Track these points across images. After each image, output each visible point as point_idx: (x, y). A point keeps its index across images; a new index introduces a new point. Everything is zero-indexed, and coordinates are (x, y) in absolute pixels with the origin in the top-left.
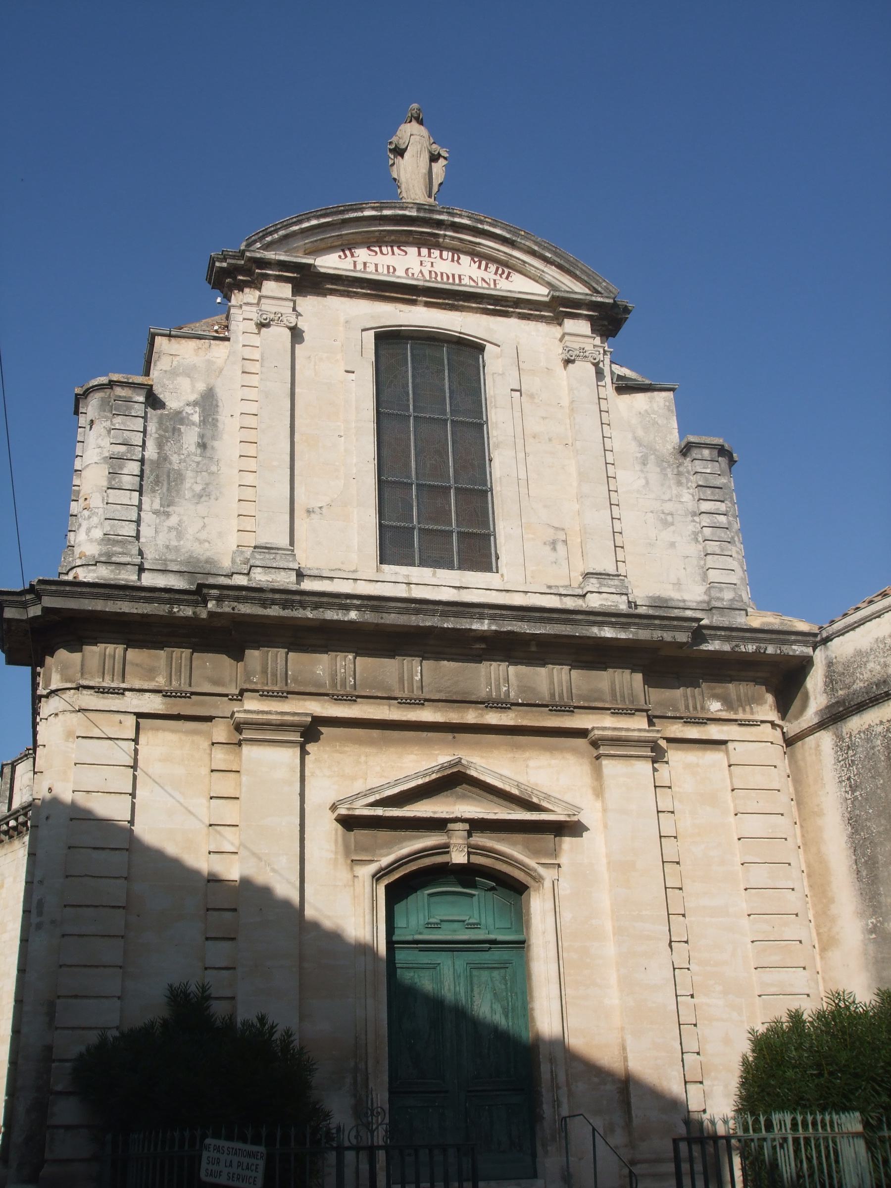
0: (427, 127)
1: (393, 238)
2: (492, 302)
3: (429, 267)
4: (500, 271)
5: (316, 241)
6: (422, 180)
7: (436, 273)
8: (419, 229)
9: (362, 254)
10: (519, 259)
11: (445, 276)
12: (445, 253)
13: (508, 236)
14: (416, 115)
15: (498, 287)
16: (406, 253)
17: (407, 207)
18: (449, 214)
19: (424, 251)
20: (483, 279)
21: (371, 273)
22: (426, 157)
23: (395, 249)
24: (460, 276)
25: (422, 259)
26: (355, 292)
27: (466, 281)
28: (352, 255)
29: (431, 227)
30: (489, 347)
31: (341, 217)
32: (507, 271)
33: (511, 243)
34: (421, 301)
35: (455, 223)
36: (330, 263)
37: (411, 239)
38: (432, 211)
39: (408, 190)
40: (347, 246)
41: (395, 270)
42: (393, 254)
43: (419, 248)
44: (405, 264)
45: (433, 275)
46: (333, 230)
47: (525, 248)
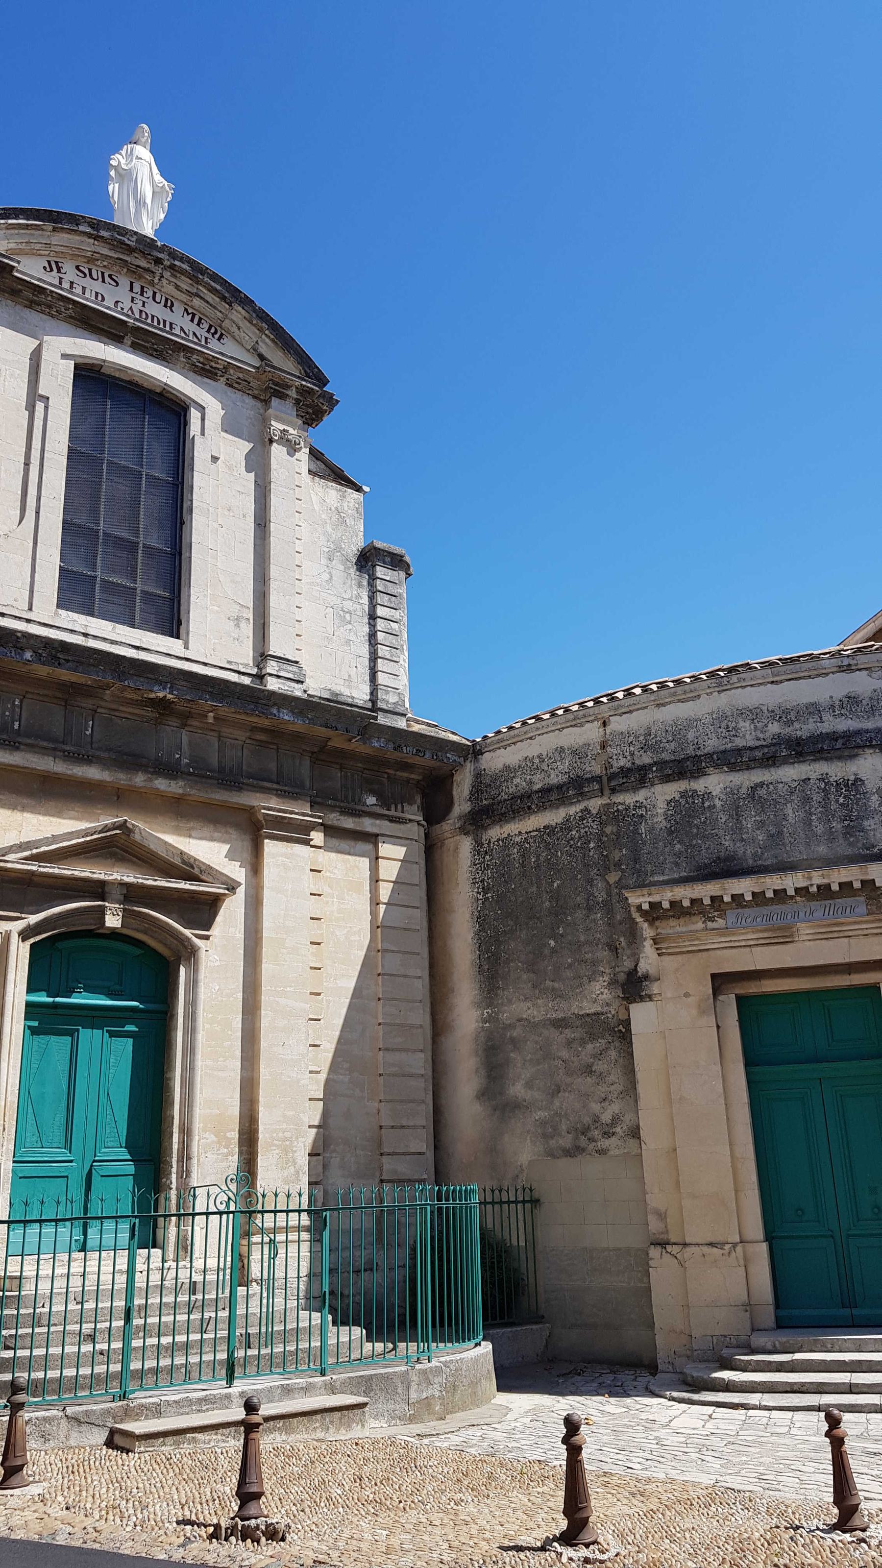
7: (146, 314)
20: (194, 334)
25: (134, 295)
41: (103, 299)
45: (144, 316)
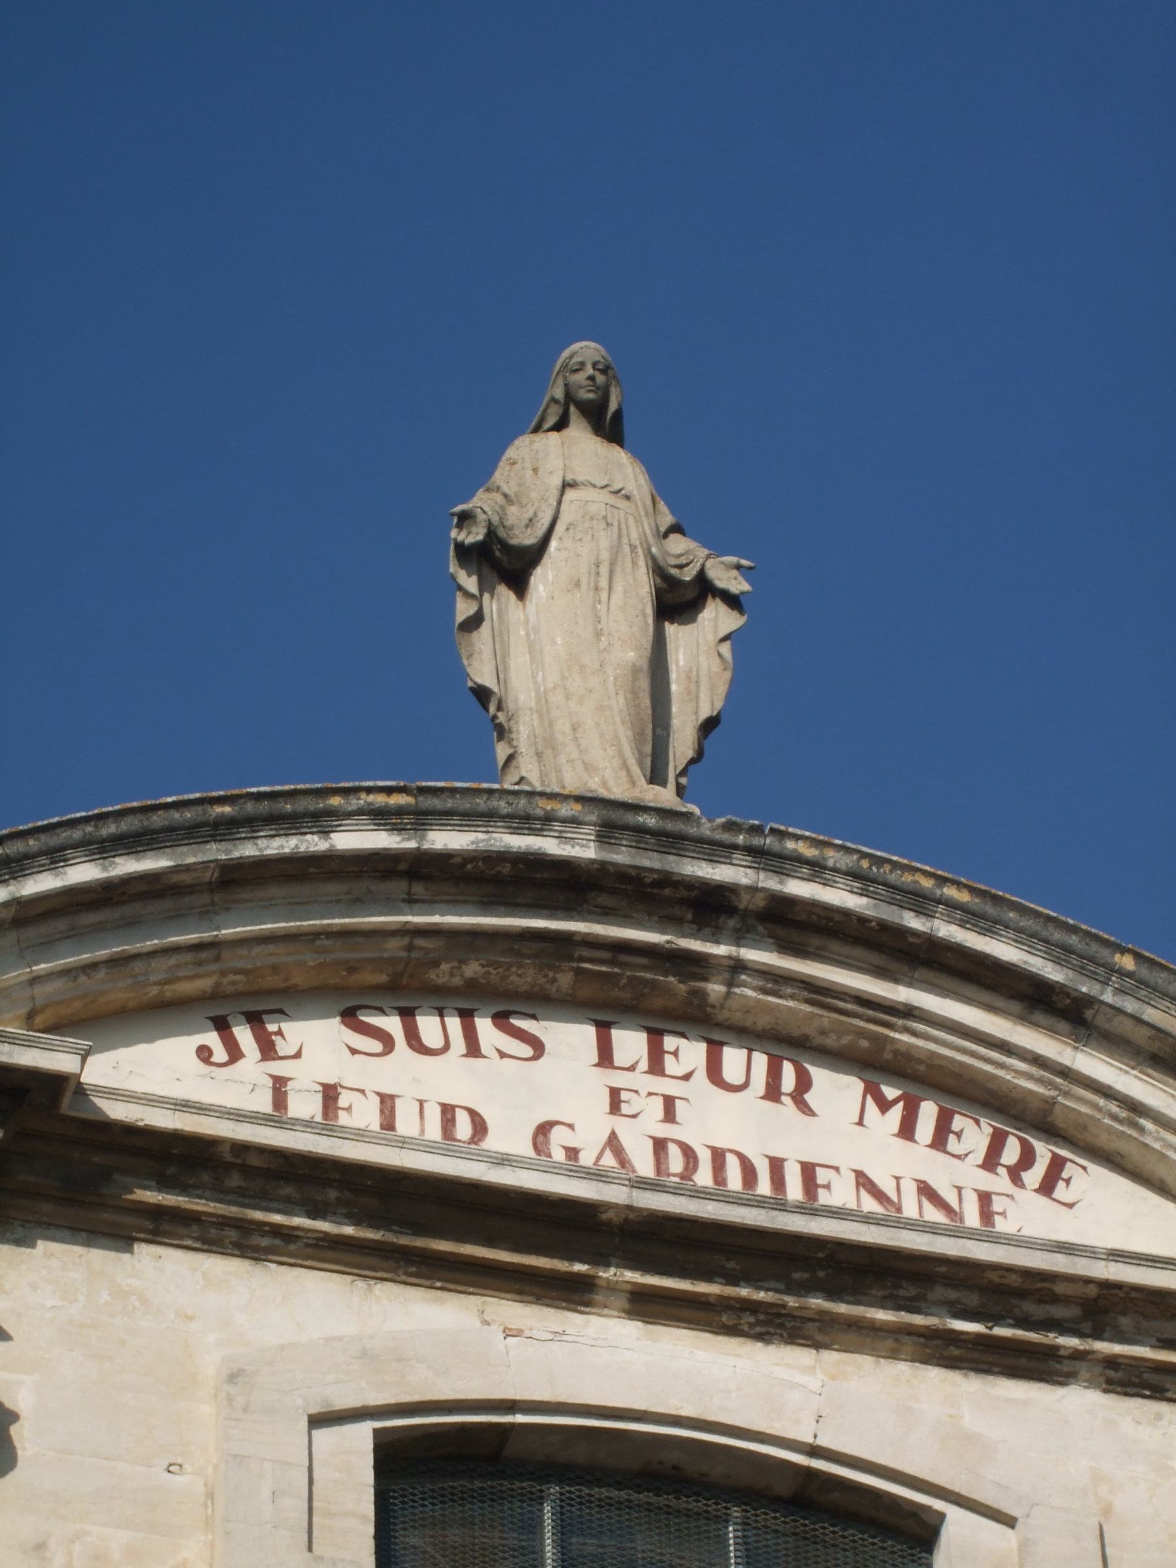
0: (639, 455)
1: (472, 969)
2: (972, 1299)
3: (652, 1121)
4: (1011, 1153)
5: (91, 967)
6: (619, 702)
7: (688, 1153)
8: (599, 930)
9: (317, 1046)
10: (1107, 1092)
11: (732, 1163)
12: (733, 1059)
13: (1053, 973)
14: (586, 395)
15: (1001, 1225)
16: (538, 1048)
17: (548, 819)
18: (761, 857)
19: (630, 1043)
20: (926, 1191)
21: (360, 1135)
22: (636, 592)
23: (484, 1026)
24: (808, 1171)
25: (619, 1079)
26: (276, 1231)
27: (840, 1192)
28: (268, 1050)
29: (668, 921)
30: (958, 1526)
31: (216, 852)
32: (1043, 1151)
33: (1068, 1012)
34: (612, 1288)
35: (791, 902)
36: (154, 1077)
37: (565, 980)
38: (673, 841)
39: (547, 747)
40: (245, 1002)
41: (480, 1127)
42: (473, 1049)
43: (603, 1028)
44: (539, 1099)
45: (676, 1162)
46: (177, 918)
47: (1140, 1036)
